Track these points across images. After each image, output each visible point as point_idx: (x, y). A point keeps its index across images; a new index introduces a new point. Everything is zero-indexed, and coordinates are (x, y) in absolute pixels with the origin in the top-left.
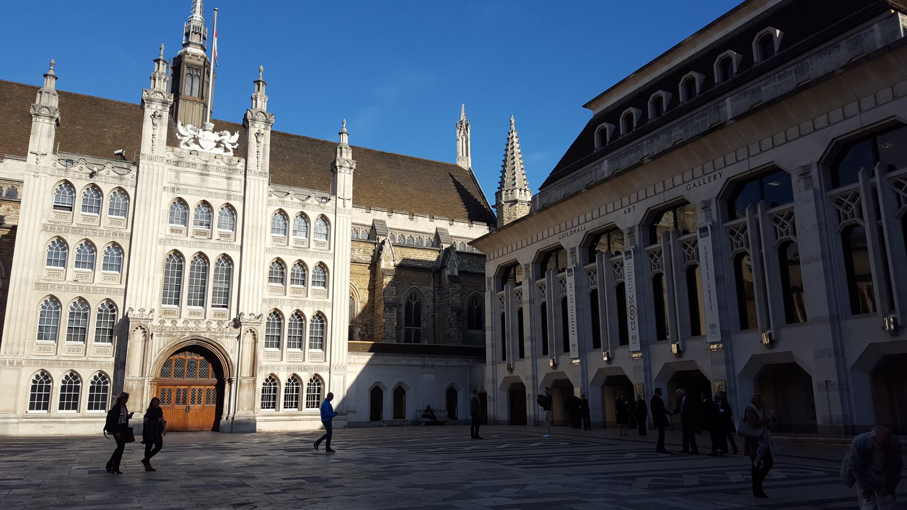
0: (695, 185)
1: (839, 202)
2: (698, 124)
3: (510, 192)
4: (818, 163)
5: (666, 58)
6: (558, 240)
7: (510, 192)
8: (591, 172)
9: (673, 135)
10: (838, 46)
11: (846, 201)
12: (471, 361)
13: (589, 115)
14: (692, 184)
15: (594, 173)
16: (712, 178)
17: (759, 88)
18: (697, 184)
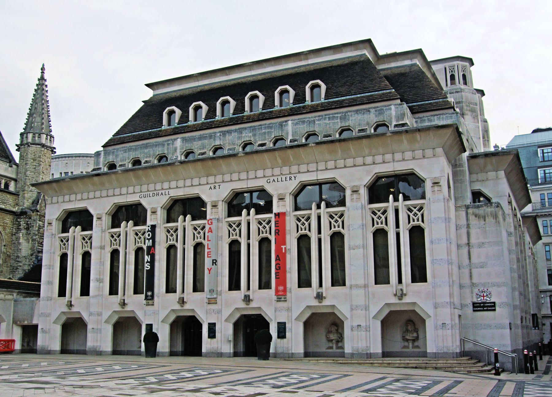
0: (274, 180)
1: (374, 213)
2: (265, 133)
3: (37, 135)
4: (365, 186)
5: (227, 71)
6: (138, 199)
7: (37, 135)
8: (163, 145)
9: (243, 135)
10: (369, 111)
11: (379, 213)
12: (15, 295)
13: (149, 94)
14: (272, 179)
15: (166, 146)
16: (288, 179)
17: (314, 121)
18: (276, 181)
